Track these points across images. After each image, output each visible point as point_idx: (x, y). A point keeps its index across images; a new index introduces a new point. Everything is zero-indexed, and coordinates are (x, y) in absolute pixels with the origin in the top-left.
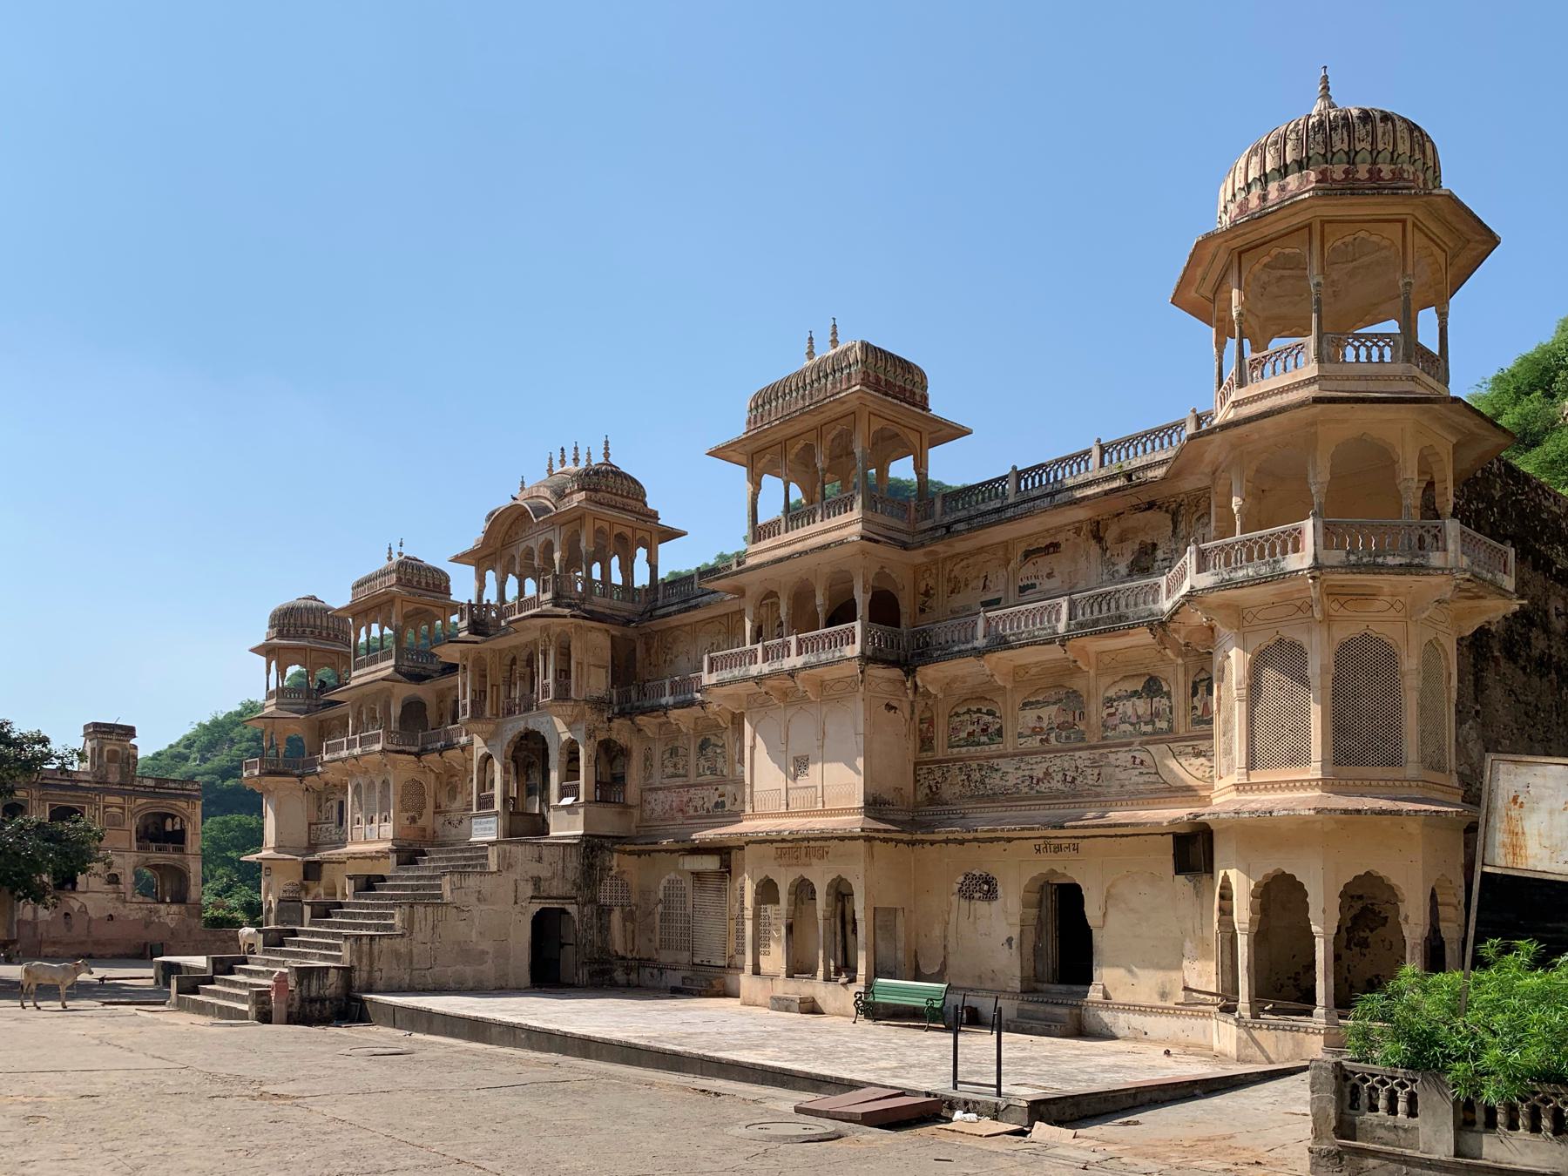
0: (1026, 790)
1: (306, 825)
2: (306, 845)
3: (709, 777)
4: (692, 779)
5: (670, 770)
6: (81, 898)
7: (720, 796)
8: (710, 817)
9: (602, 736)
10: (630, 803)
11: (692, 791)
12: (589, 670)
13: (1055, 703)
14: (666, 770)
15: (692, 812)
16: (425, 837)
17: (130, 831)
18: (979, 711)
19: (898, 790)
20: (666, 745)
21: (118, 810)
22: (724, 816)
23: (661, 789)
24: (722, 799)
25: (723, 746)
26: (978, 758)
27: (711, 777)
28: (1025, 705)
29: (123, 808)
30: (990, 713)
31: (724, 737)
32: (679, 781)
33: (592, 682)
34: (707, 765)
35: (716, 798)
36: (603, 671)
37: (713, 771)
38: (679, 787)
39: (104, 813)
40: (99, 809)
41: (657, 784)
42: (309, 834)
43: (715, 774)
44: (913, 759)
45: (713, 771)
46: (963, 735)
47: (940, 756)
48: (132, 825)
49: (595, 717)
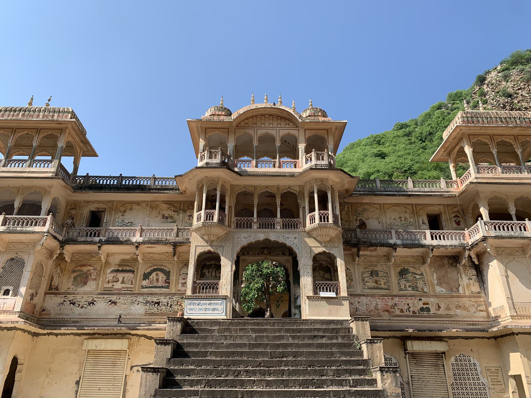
3: (410, 291)
4: (395, 291)
5: (372, 284)
7: (424, 304)
8: (417, 317)
11: (396, 299)
14: (368, 284)
15: (398, 312)
20: (366, 268)
22: (430, 317)
23: (364, 295)
24: (427, 306)
25: (422, 274)
27: (412, 292)
31: (421, 269)
32: (383, 292)
34: (408, 284)
35: (421, 305)
37: (415, 288)
38: (383, 296)
41: (359, 292)
43: (417, 290)
45: (415, 288)
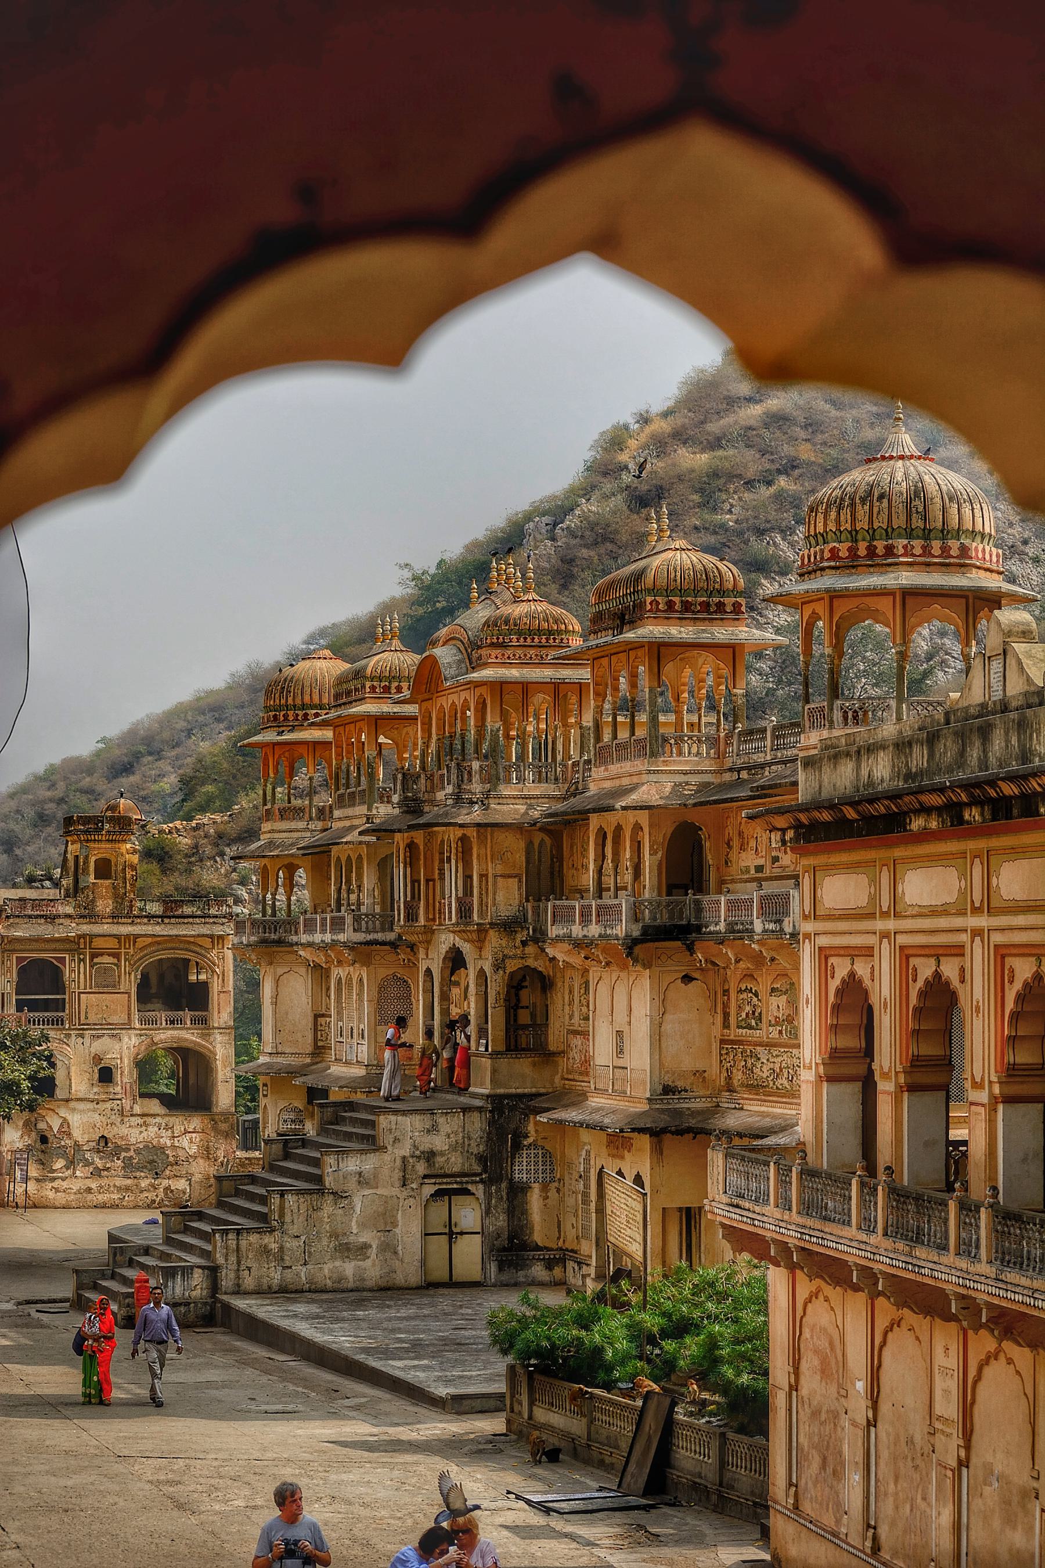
0: (771, 1083)
1: (311, 1019)
2: (309, 1049)
6: (63, 1112)
9: (512, 966)
10: (552, 1048)
12: (495, 884)
13: (785, 994)
16: (410, 1059)
17: (129, 994)
18: (751, 991)
19: (699, 1074)
21: (111, 960)
26: (749, 1043)
28: (773, 990)
29: (117, 956)
30: (756, 995)
33: (500, 897)
36: (513, 883)
39: (91, 966)
40: (84, 960)
42: (316, 1030)
44: (719, 1037)
46: (744, 1016)
47: (732, 1037)
48: (130, 983)
49: (504, 943)
